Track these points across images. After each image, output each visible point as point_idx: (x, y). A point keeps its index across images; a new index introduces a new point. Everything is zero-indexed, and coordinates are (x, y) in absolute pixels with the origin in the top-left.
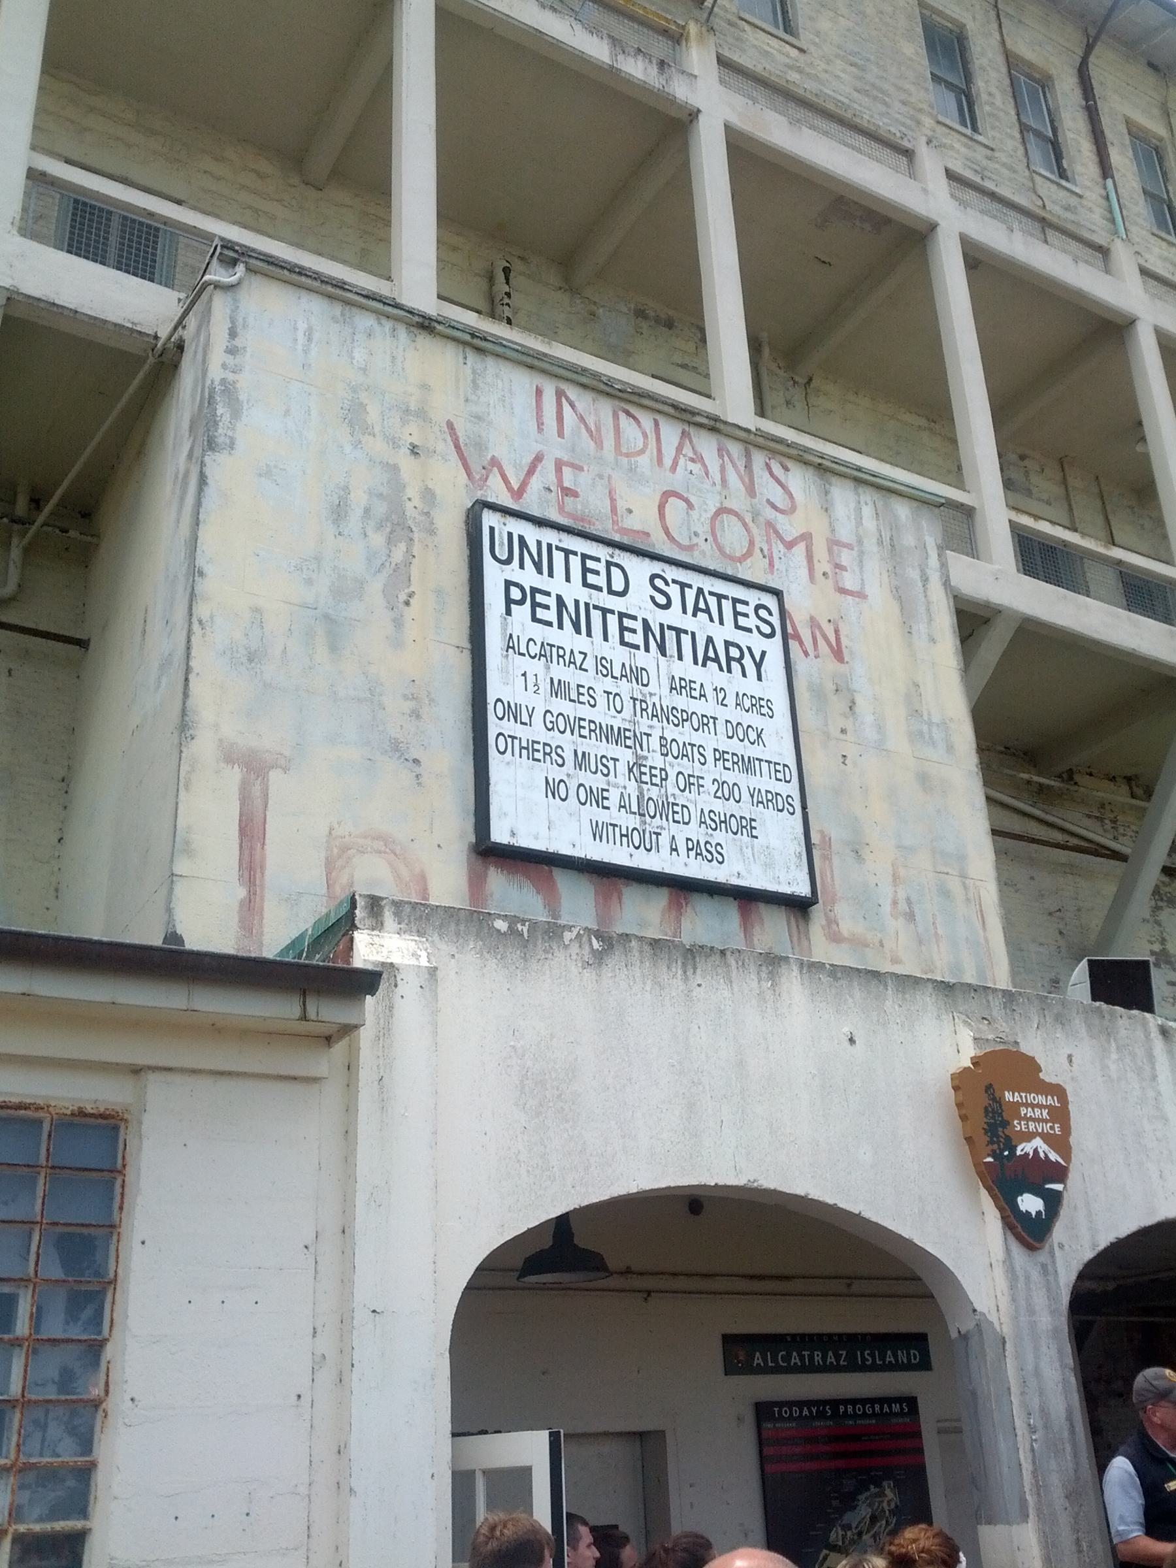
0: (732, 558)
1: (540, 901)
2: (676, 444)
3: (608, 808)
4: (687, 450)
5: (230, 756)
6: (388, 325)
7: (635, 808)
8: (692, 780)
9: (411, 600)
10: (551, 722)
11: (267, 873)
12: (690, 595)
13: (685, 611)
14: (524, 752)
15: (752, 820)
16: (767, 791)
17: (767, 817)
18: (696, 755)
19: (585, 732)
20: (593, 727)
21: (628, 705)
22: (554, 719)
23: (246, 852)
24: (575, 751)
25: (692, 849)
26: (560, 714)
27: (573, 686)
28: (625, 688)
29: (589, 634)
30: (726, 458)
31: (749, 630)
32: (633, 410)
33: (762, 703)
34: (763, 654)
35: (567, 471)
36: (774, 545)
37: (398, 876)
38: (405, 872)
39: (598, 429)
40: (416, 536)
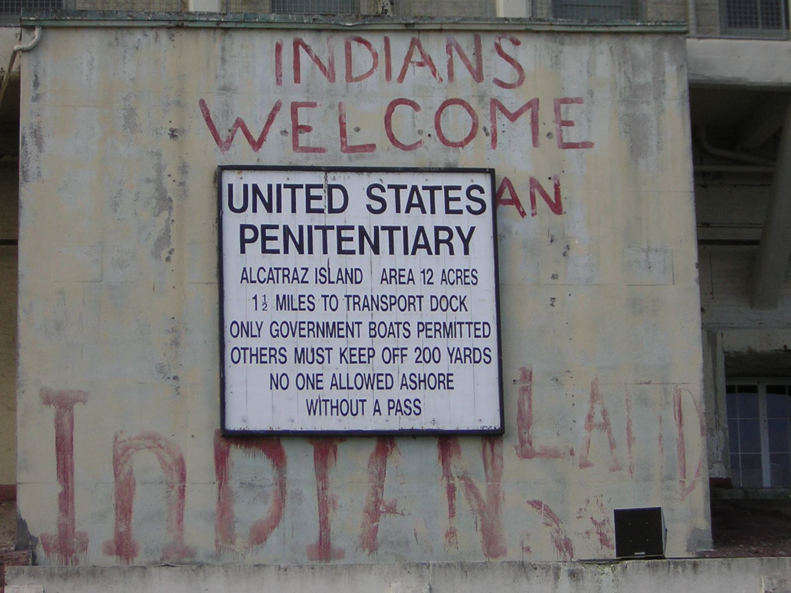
0: (455, 145)
1: (270, 462)
2: (405, 53)
3: (322, 388)
4: (417, 57)
5: (48, 399)
6: (151, 34)
7: (344, 385)
8: (396, 352)
9: (171, 256)
10: (276, 330)
11: (75, 473)
12: (405, 195)
13: (398, 210)
14: (254, 358)
15: (448, 375)
16: (465, 349)
17: (462, 372)
18: (402, 330)
19: (303, 333)
20: (311, 326)
22: (279, 328)
23: (61, 462)
24: (296, 350)
25: (393, 408)
26: (285, 322)
27: (296, 298)
28: (340, 290)
29: (311, 251)
30: (455, 53)
31: (460, 212)
32: (365, 36)
33: (467, 273)
35: (301, 111)
36: (498, 120)
37: (163, 462)
38: (168, 459)
39: (331, 64)
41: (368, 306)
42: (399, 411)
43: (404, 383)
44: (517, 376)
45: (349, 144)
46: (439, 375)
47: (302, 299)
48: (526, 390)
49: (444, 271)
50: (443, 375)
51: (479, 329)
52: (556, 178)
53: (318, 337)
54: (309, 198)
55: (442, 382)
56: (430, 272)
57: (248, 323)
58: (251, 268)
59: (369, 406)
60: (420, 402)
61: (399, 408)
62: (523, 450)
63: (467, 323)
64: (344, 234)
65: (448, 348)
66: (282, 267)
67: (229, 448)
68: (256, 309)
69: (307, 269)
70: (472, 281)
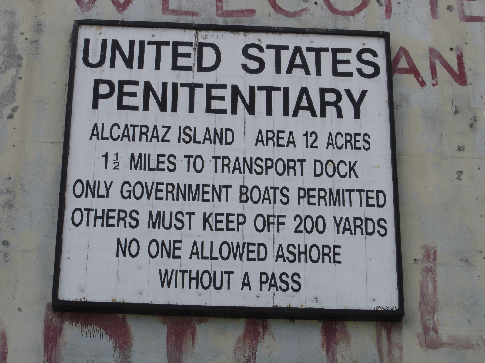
0: (344, 14)
3: (179, 257)
7: (207, 253)
8: (271, 220)
10: (128, 191)
14: (99, 221)
15: (335, 247)
16: (355, 219)
19: (160, 195)
20: (170, 188)
21: (209, 164)
22: (131, 189)
24: (151, 213)
25: (266, 282)
31: (350, 75)
33: (358, 138)
34: (364, 93)
40: (24, 62)
41: (239, 169)
42: (273, 286)
43: (280, 254)
44: (419, 254)
45: (225, 9)
46: (324, 246)
47: (161, 159)
48: (429, 270)
49: (330, 134)
50: (328, 246)
51: (372, 198)
52: (458, 49)
53: (178, 199)
54: (176, 55)
55: (328, 255)
56: (314, 135)
57: (95, 182)
58: (103, 125)
59: (237, 279)
60: (299, 277)
61: (273, 283)
62: (427, 338)
63: (357, 191)
64: (215, 92)
65: (335, 218)
66: (140, 124)
67: (62, 325)
68: (106, 168)
69: (169, 128)
70: (363, 146)
